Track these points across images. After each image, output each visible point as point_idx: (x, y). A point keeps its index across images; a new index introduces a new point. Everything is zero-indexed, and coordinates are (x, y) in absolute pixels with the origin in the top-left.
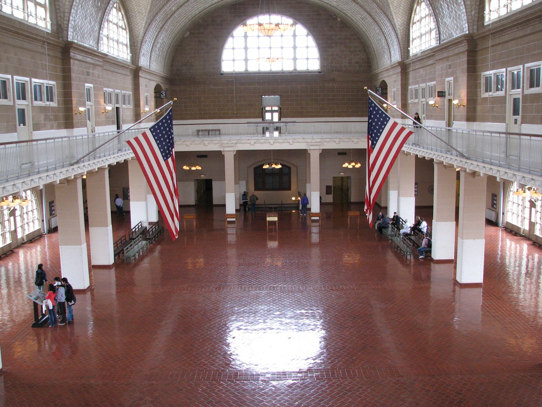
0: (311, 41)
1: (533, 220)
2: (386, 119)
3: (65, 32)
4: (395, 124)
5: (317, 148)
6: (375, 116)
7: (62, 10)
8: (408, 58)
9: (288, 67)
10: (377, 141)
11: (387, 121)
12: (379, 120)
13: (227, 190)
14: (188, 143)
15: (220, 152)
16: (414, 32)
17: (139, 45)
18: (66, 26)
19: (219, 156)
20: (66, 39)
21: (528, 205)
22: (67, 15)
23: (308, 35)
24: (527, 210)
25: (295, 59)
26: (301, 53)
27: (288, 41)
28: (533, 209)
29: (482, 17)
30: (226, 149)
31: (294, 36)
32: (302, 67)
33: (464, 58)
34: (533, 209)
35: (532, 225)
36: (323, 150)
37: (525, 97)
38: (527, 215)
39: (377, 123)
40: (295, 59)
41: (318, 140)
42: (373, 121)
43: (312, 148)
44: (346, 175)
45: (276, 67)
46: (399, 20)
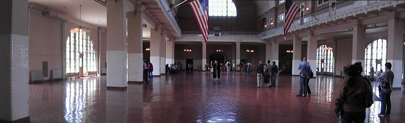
4: (295, 5)
5: (239, 41)
9: (225, 15)
10: (288, 10)
11: (292, 3)
13: (203, 57)
14: (188, 38)
15: (201, 42)
19: (199, 45)
21: (320, 62)
24: (320, 65)
32: (230, 15)
35: (322, 69)
36: (242, 42)
38: (320, 67)
43: (237, 41)
45: (220, 15)
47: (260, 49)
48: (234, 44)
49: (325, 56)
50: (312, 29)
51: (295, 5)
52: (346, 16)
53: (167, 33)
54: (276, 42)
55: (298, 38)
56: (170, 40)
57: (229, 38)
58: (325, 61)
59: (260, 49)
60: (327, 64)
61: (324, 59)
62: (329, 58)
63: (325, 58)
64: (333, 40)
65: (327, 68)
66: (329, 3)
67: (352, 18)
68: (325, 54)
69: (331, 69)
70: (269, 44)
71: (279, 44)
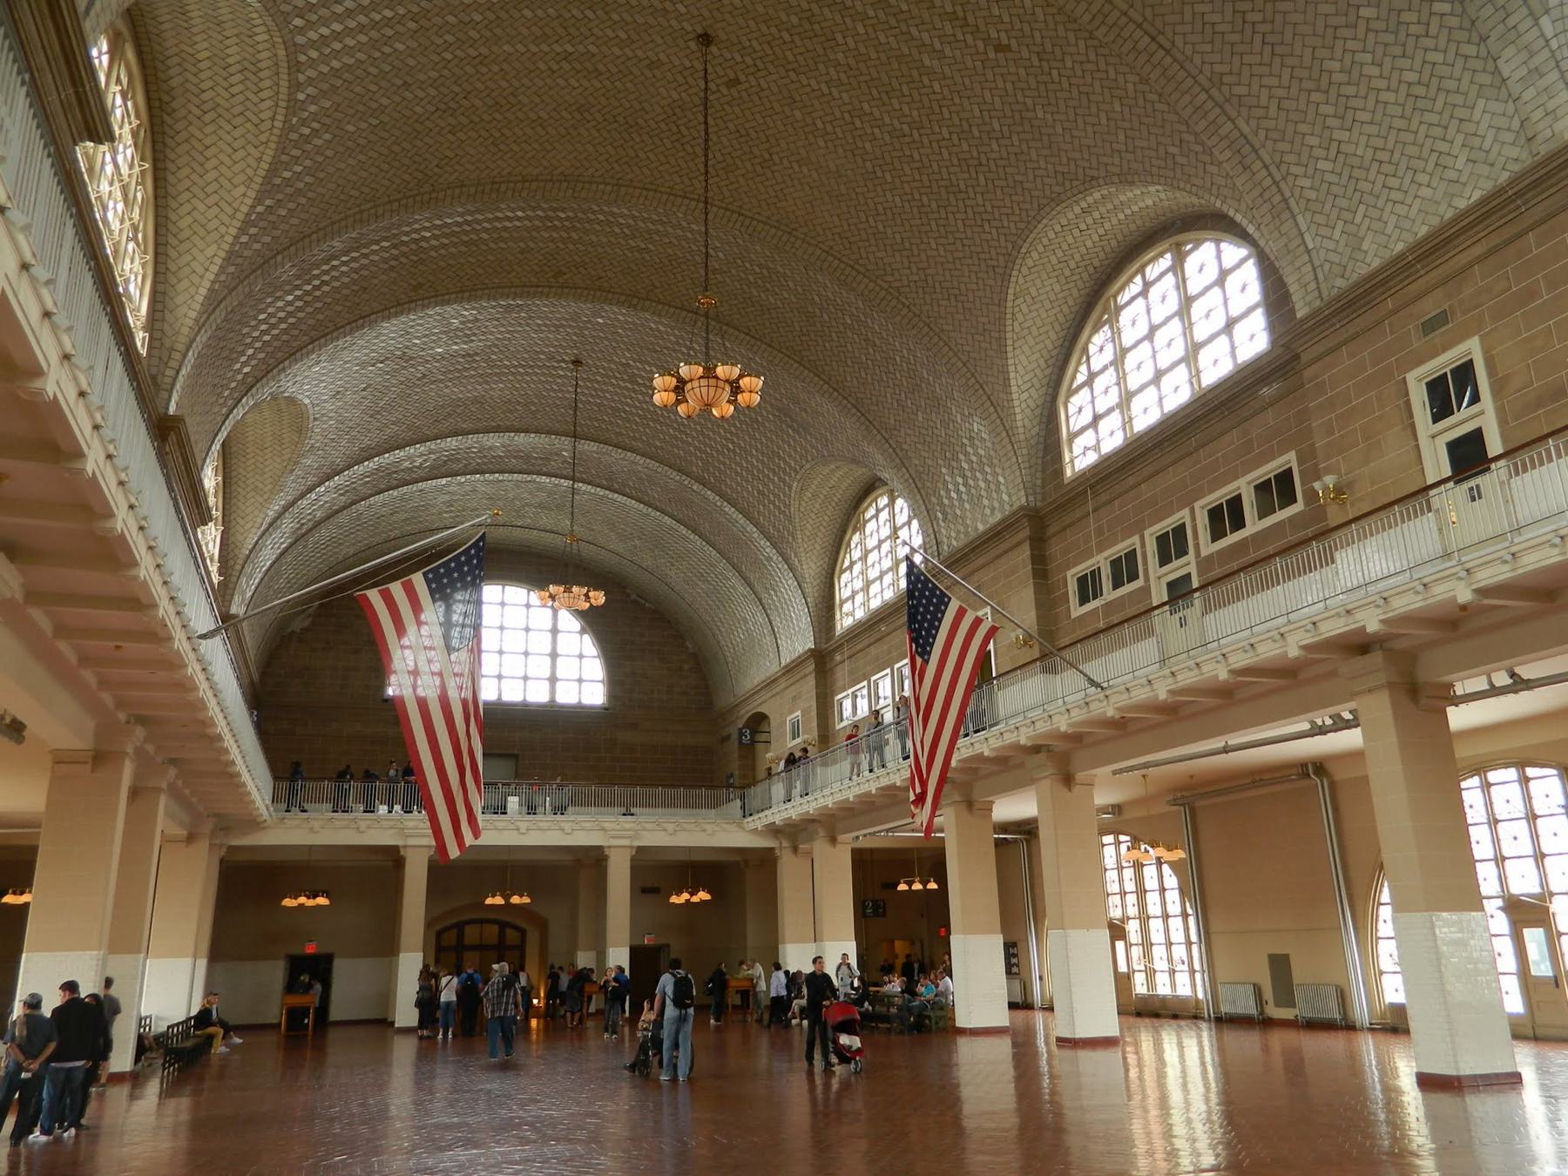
0: (589, 645)
1: (1123, 968)
2: (943, 601)
3: (165, 395)
4: (961, 613)
6: (922, 595)
7: (167, 343)
8: (828, 640)
9: (538, 694)
11: (947, 605)
12: (929, 602)
14: (316, 825)
16: (847, 584)
17: (238, 567)
18: (168, 380)
20: (162, 411)
22: (177, 356)
23: (583, 631)
25: (553, 680)
26: (566, 668)
27: (542, 642)
28: (1120, 945)
29: (1060, 472)
30: (411, 842)
31: (555, 631)
32: (567, 696)
33: (1025, 552)
34: (1120, 945)
36: (640, 849)
37: (1204, 564)
39: (926, 607)
40: (553, 680)
41: (627, 826)
42: (920, 603)
44: (662, 941)
46: (811, 567)
47: (739, 882)
48: (593, 861)
49: (1131, 899)
50: (1060, 746)
51: (961, 613)
52: (1309, 639)
53: (174, 792)
54: (833, 840)
55: (970, 805)
56: (191, 838)
57: (567, 827)
58: (1133, 927)
59: (739, 882)
60: (1147, 945)
61: (1125, 919)
62: (1154, 908)
63: (1132, 911)
64: (1175, 802)
65: (1151, 973)
66: (1146, 590)
67: (1358, 645)
68: (1130, 886)
69: (1183, 980)
70: (795, 850)
71: (854, 851)
